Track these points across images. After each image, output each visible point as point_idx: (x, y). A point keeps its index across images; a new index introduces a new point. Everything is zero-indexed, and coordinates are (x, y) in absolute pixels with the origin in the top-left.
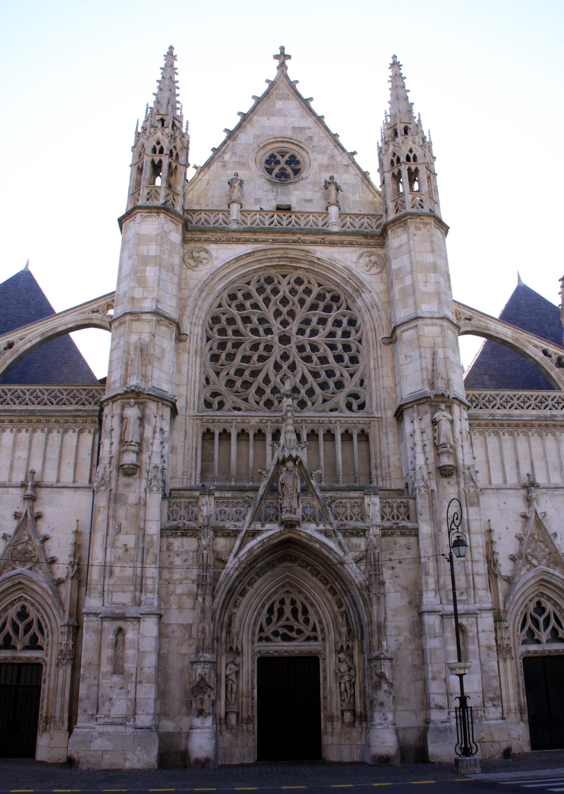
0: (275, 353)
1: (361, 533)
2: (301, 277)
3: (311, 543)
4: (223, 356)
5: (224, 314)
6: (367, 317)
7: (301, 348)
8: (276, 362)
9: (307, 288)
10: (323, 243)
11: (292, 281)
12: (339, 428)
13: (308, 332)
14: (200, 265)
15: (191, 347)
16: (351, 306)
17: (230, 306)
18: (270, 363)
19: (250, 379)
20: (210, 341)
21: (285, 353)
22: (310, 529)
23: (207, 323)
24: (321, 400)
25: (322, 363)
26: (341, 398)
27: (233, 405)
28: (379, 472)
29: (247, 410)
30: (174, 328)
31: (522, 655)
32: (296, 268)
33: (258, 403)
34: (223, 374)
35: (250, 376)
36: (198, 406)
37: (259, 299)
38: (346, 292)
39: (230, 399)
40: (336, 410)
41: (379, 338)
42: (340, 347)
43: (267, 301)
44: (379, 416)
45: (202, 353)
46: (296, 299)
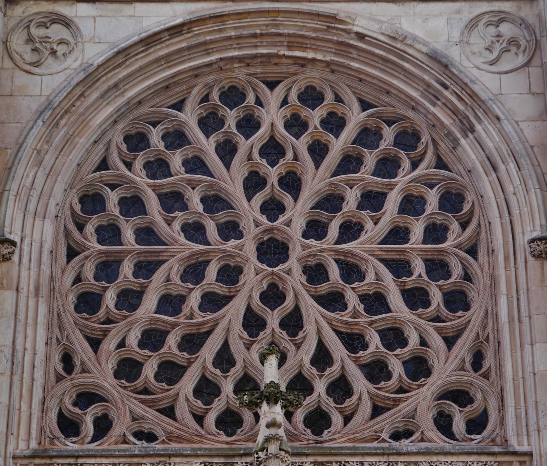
0: (246, 289)
2: (317, 83)
4: (110, 298)
5: (113, 187)
6: (486, 185)
7: (315, 273)
8: (249, 309)
9: (331, 114)
11: (293, 97)
13: (334, 230)
14: (50, 60)
15: (24, 274)
16: (448, 158)
17: (129, 165)
18: (235, 311)
19: (181, 357)
21: (273, 286)
24: (366, 408)
25: (370, 310)
26: (423, 400)
27: (135, 427)
29: (171, 438)
32: (303, 63)
33: (199, 419)
34: (110, 344)
35: (181, 347)
36: (42, 429)
37: (208, 146)
38: (435, 124)
39: (125, 407)
40: (408, 434)
41: (522, 240)
42: (419, 267)
43: (227, 151)
44: (525, 448)
45: (52, 289)
46: (302, 144)
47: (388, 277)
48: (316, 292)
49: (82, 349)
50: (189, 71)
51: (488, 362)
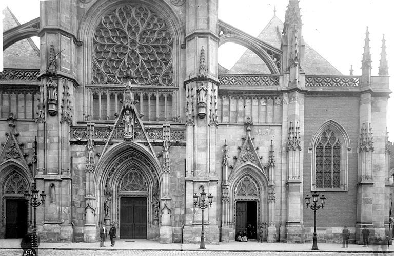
31: (236, 200)
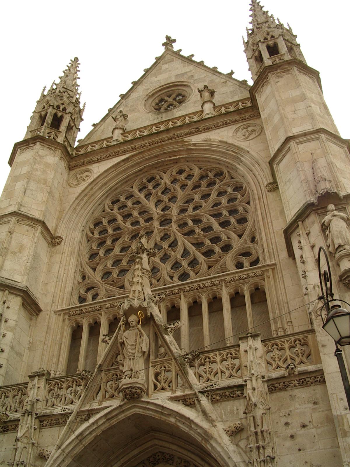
1: (236, 392)
3: (164, 418)
10: (198, 131)
12: (224, 288)
17: (112, 210)
20: (89, 242)
22: (162, 398)
23: (88, 229)
26: (229, 259)
28: (279, 325)
30: (39, 228)
34: (100, 268)
37: (141, 196)
47: (212, 220)
48: (183, 231)
49: (89, 271)
50: (133, 174)
51: (257, 237)
